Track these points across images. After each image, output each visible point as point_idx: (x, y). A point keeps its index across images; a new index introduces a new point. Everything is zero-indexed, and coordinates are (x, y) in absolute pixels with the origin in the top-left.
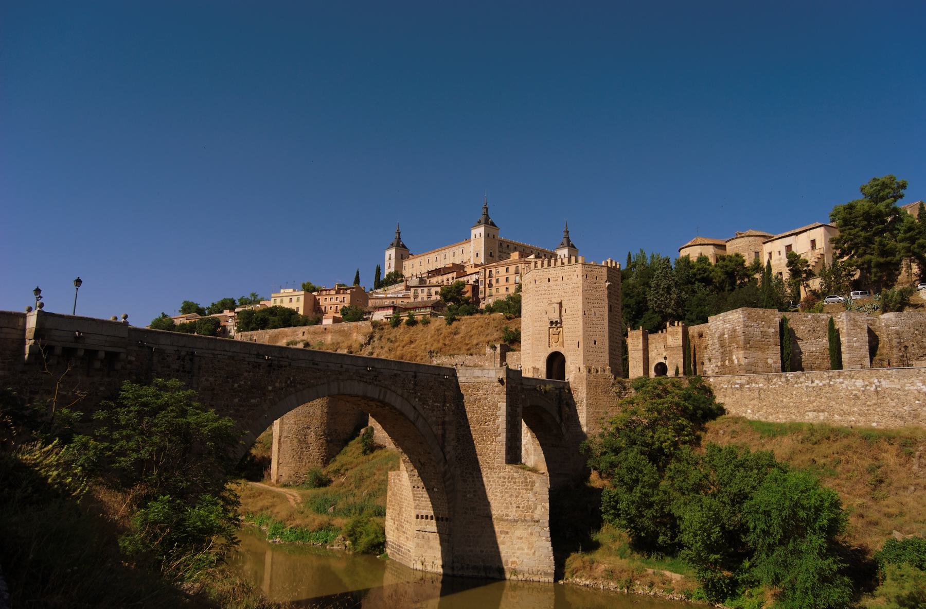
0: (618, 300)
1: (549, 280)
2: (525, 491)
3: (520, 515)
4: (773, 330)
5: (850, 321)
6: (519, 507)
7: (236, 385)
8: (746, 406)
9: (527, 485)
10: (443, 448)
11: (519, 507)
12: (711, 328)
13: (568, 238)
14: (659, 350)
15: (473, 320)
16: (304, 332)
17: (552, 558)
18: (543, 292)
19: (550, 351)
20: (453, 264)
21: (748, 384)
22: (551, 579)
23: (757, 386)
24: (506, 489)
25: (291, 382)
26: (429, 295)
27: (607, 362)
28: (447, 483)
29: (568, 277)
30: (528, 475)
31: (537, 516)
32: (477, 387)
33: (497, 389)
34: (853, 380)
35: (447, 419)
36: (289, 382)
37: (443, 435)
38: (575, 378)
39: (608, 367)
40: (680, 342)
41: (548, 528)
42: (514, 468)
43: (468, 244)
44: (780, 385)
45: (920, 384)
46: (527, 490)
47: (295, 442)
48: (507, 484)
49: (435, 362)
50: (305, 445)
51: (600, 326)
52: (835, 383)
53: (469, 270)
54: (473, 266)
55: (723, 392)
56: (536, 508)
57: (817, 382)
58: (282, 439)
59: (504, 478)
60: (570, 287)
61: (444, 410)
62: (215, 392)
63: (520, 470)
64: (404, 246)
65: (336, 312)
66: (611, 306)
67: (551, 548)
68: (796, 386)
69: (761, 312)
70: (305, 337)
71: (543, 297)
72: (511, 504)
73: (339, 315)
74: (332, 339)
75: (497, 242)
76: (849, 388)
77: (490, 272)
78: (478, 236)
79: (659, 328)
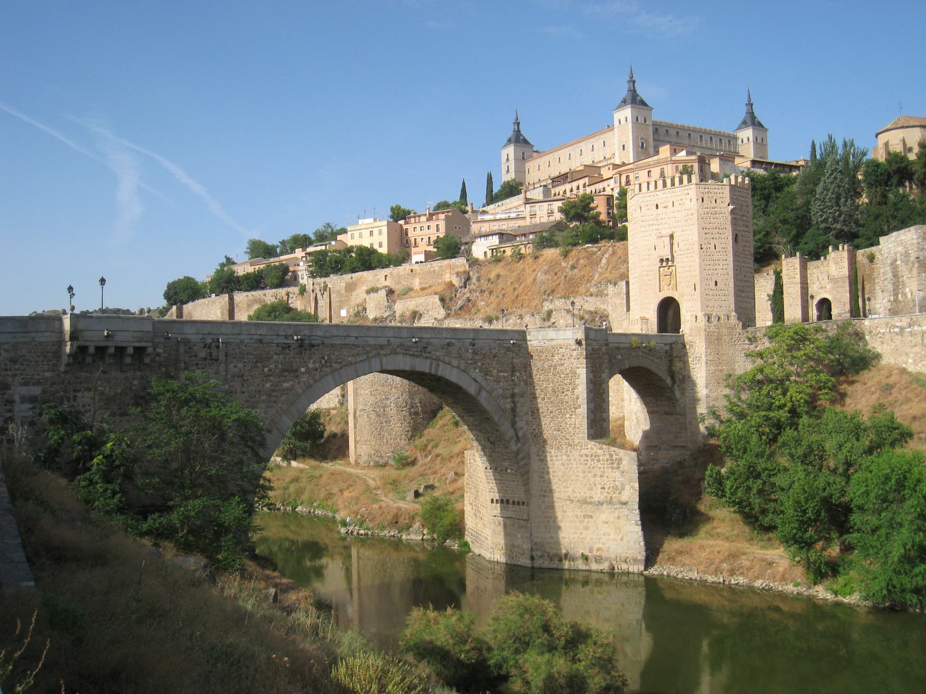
0: (747, 227)
2: (610, 470)
3: (606, 497)
6: (604, 488)
7: (266, 369)
8: (907, 354)
9: (612, 463)
10: (513, 424)
11: (604, 488)
12: (883, 252)
13: (753, 113)
14: (822, 282)
15: (595, 249)
16: (386, 276)
17: (642, 543)
18: (651, 222)
20: (585, 166)
21: (910, 326)
22: (642, 568)
23: (920, 329)
24: (589, 468)
25: (325, 362)
26: (551, 213)
27: (733, 306)
30: (614, 451)
31: (625, 497)
32: (552, 351)
33: (575, 353)
35: (517, 390)
36: (323, 362)
37: (513, 410)
38: (691, 330)
39: (734, 314)
40: (845, 271)
41: (638, 511)
42: (597, 444)
43: (611, 133)
46: (612, 468)
47: (373, 416)
48: (590, 462)
49: (497, 326)
50: (385, 420)
51: (722, 263)
53: (606, 173)
54: (611, 167)
55: (880, 337)
56: (623, 489)
58: (358, 413)
59: (587, 456)
60: (683, 214)
61: (513, 380)
62: (245, 378)
63: (604, 446)
64: (526, 142)
65: (429, 244)
66: (736, 235)
67: (641, 533)
70: (388, 283)
72: (595, 485)
73: (431, 249)
74: (420, 283)
75: (651, 130)
77: (628, 177)
78: (623, 121)
79: (816, 254)
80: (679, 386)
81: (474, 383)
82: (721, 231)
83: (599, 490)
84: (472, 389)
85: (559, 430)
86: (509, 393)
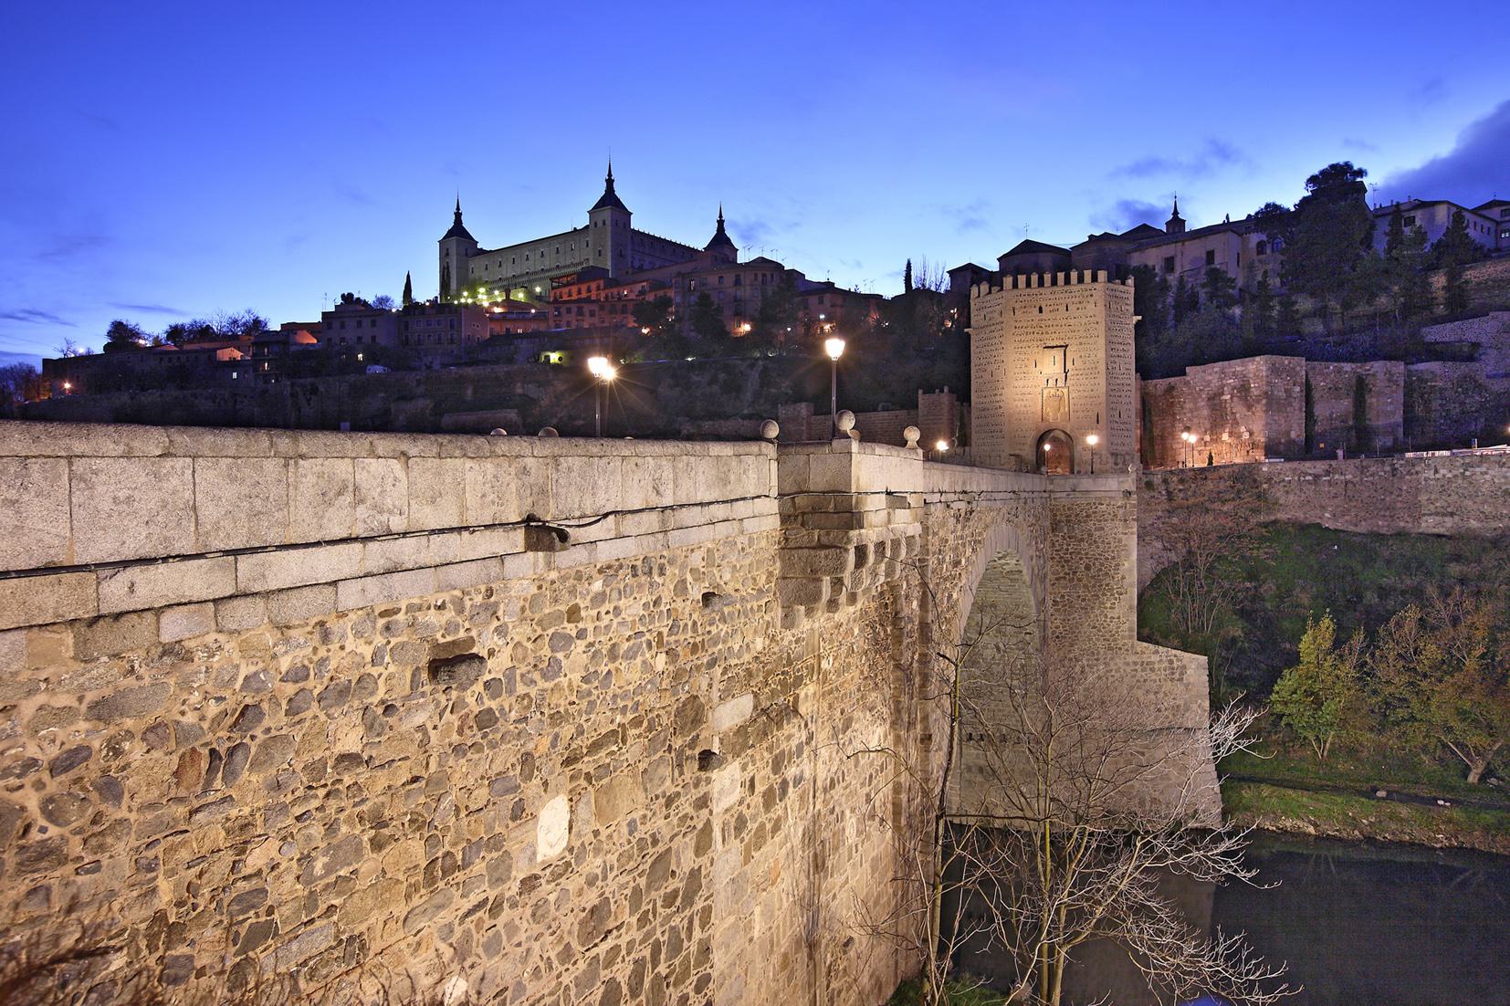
1: (1041, 310)
9: (1173, 674)
18: (1029, 330)
21: (1328, 473)
23: (1343, 478)
24: (1138, 681)
29: (1079, 306)
34: (1504, 469)
48: (1139, 674)
57: (1442, 471)
59: (1136, 664)
68: (1407, 477)
69: (1286, 362)
71: (1029, 337)
76: (1496, 481)
78: (600, 224)
85: (1094, 627)
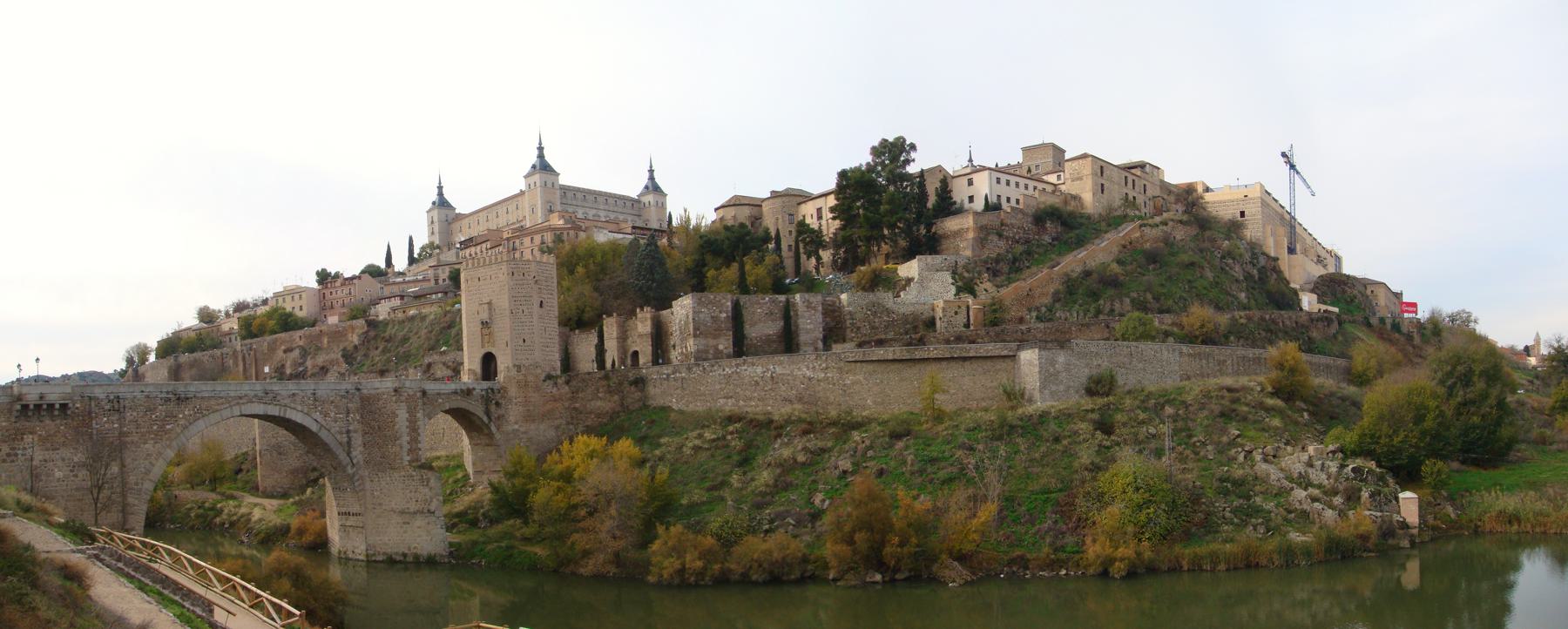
0: (552, 294)
4: (725, 315)
5: (804, 302)
8: (672, 395)
10: (349, 454)
11: (417, 501)
19: (483, 351)
28: (356, 484)
31: (432, 509)
32: (377, 397)
33: (394, 398)
35: (351, 428)
37: (349, 443)
38: (504, 378)
44: (699, 375)
45: (805, 369)
48: (406, 482)
52: (741, 370)
56: (431, 501)
57: (727, 370)
69: (712, 297)
80: (494, 423)
81: (315, 423)
82: (527, 299)
83: (415, 503)
84: (314, 428)
86: (344, 430)
